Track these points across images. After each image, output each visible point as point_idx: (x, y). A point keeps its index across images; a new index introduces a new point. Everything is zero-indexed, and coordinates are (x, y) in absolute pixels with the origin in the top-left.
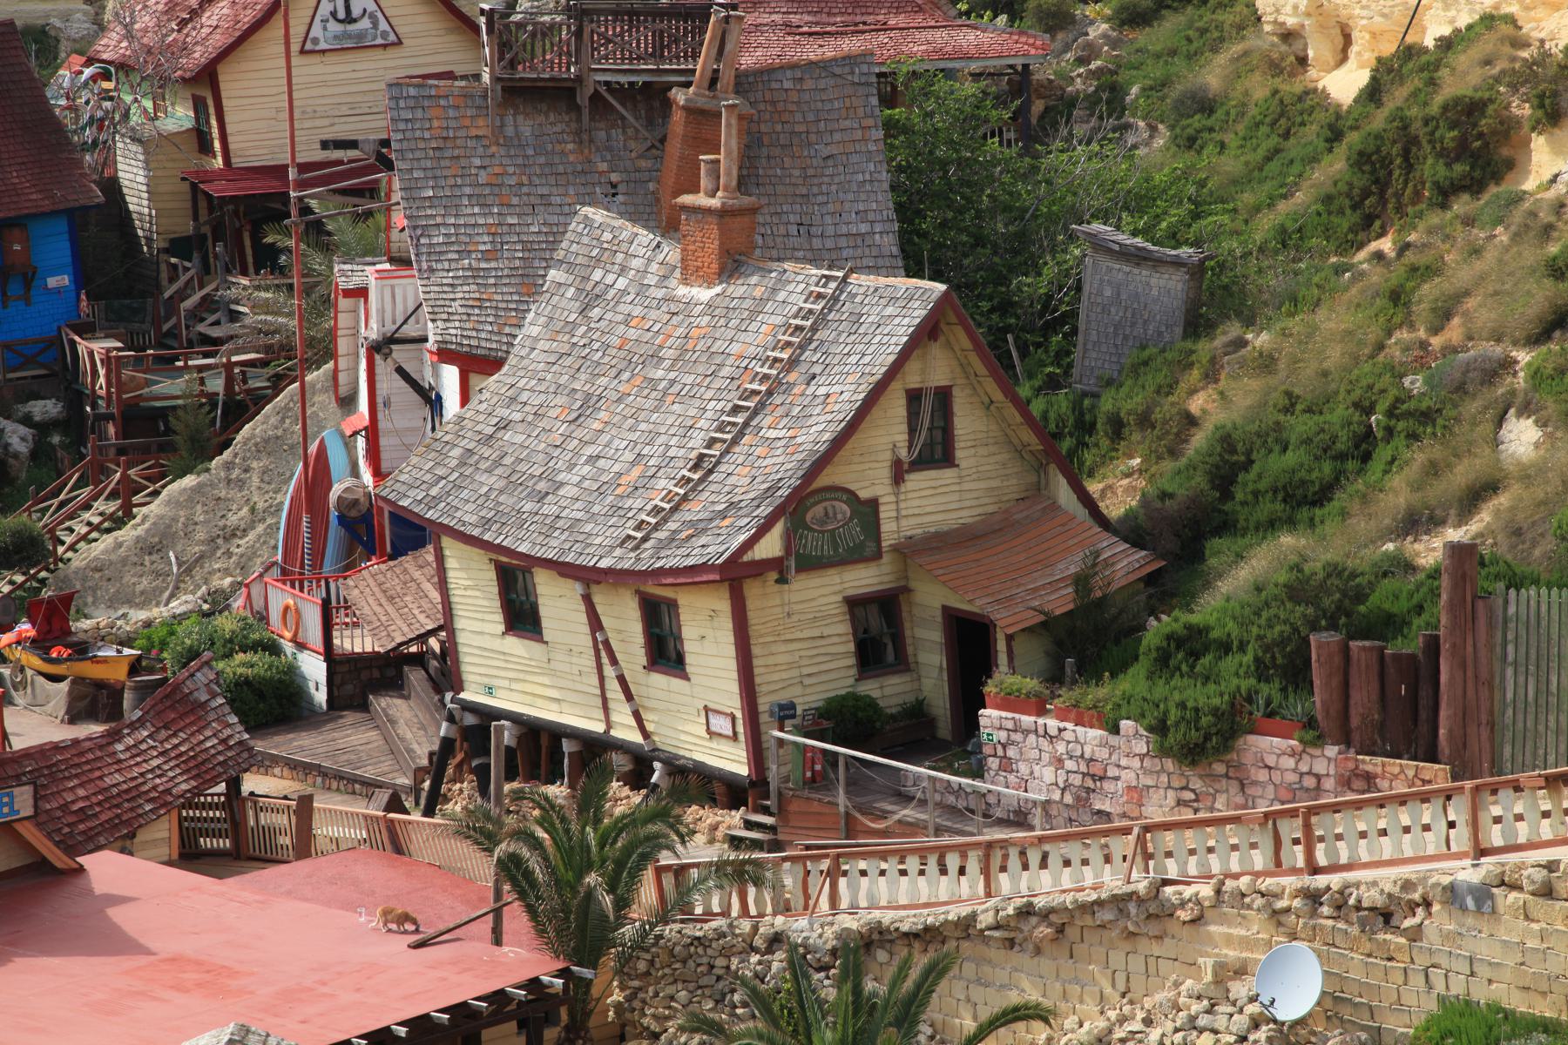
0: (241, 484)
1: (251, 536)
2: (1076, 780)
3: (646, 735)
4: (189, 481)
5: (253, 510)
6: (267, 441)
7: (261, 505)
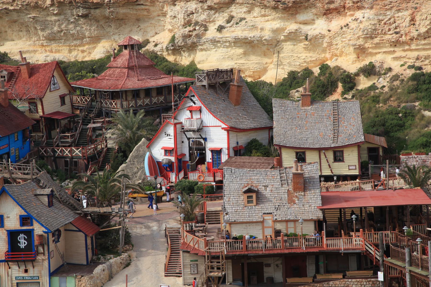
0: (134, 164)
1: (139, 173)
2: (421, 163)
3: (332, 173)
4: (123, 165)
5: (137, 168)
6: (136, 156)
7: (139, 167)
